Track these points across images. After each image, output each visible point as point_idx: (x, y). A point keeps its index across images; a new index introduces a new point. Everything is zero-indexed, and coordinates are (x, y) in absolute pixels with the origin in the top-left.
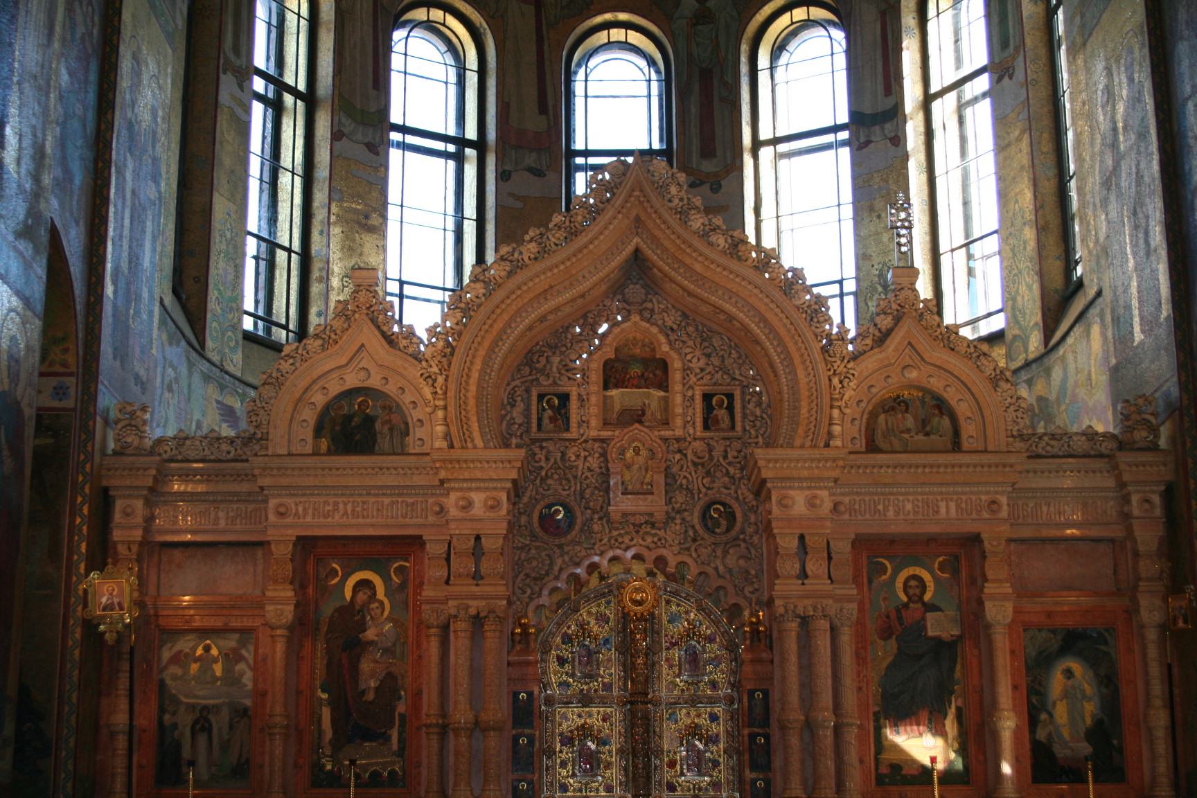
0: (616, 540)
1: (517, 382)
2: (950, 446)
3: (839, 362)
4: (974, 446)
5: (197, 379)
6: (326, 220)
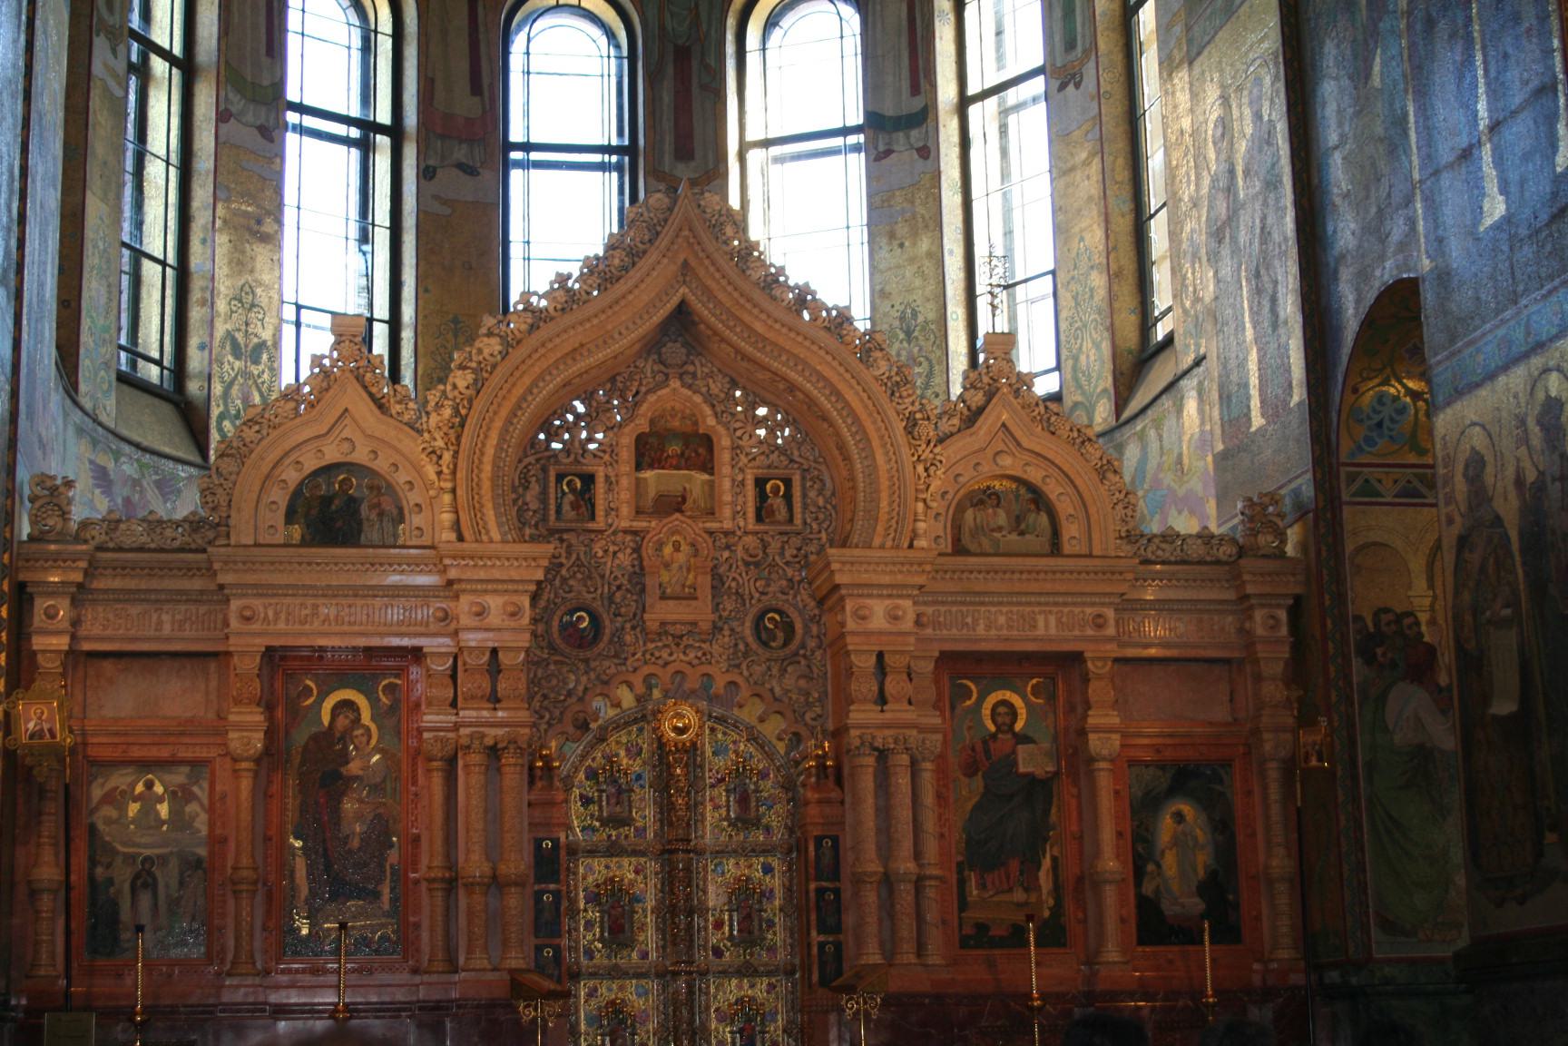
0: (652, 655)
1: (531, 459)
2: (1047, 548)
3: (924, 446)
4: (1077, 550)
5: (71, 431)
6: (210, 226)
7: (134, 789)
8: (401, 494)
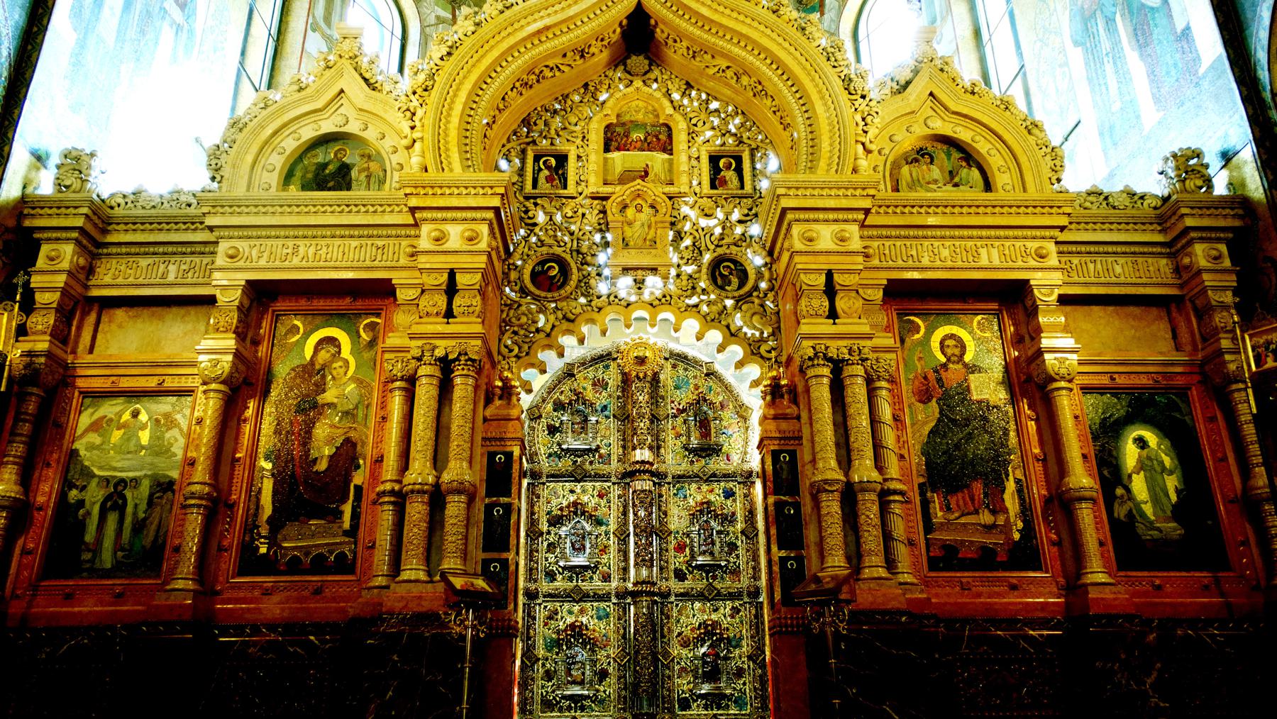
0: (616, 297)
7: (120, 417)
8: (385, 156)
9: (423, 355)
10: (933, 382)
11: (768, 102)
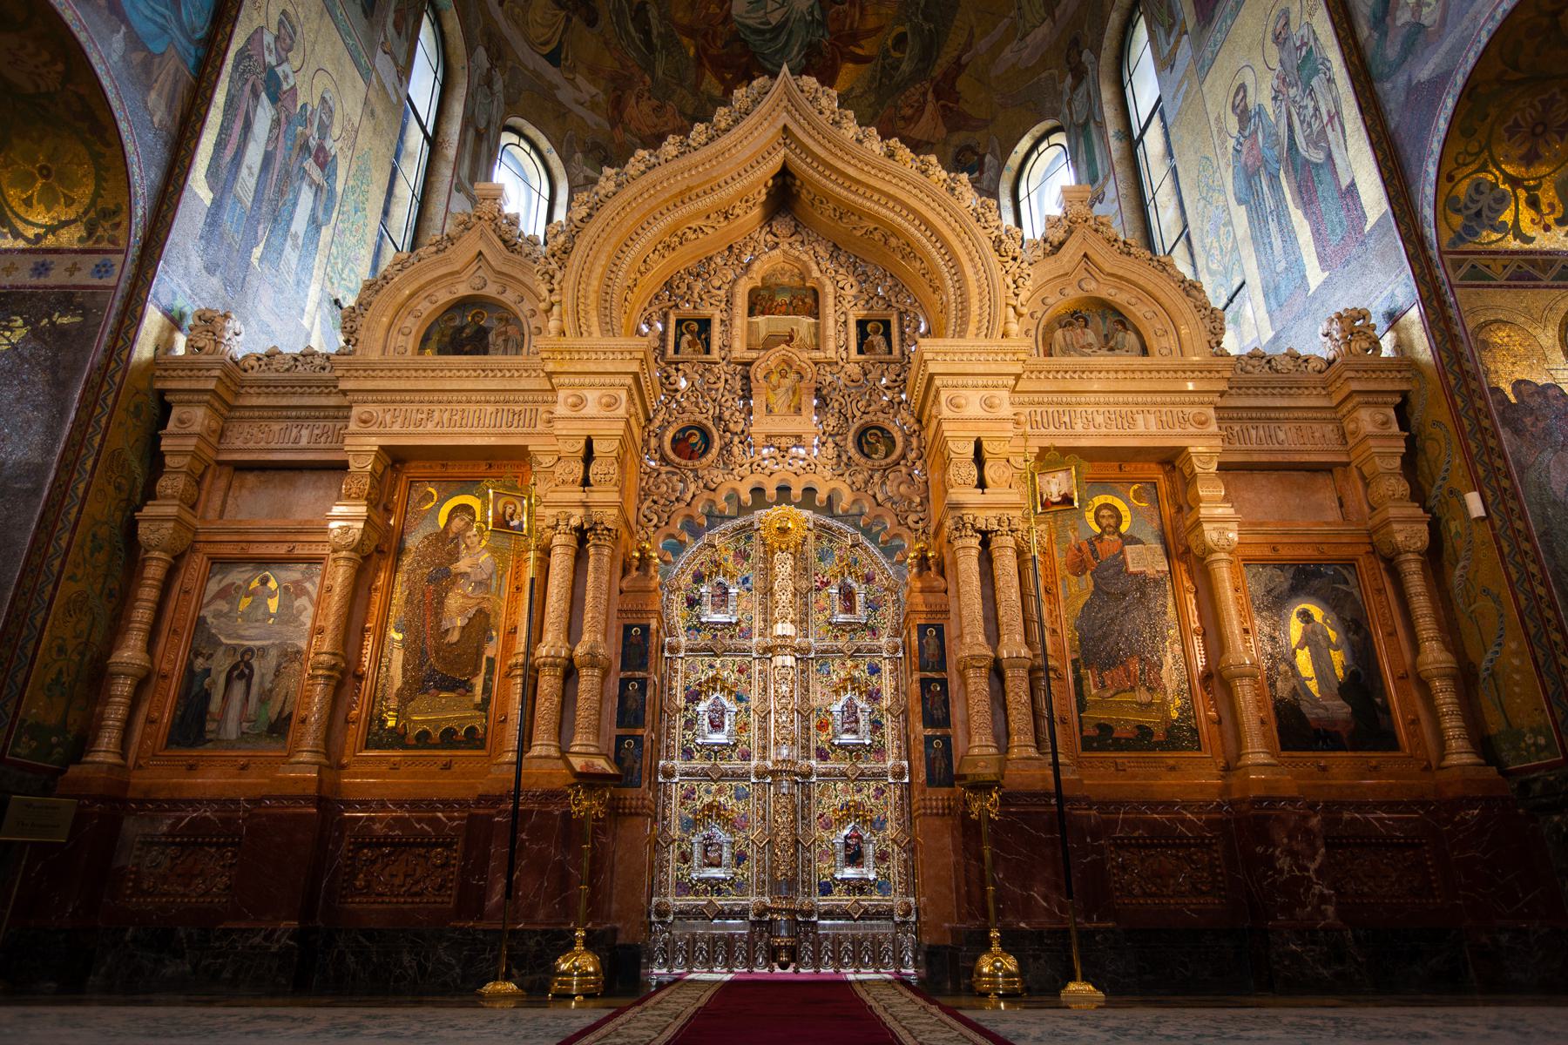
1: (654, 308)
7: (249, 584)
9: (557, 525)
10: (1087, 555)
11: (918, 264)
